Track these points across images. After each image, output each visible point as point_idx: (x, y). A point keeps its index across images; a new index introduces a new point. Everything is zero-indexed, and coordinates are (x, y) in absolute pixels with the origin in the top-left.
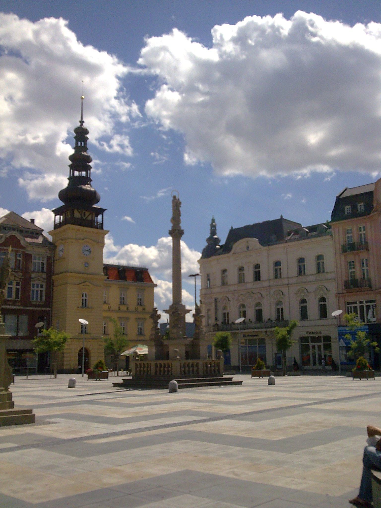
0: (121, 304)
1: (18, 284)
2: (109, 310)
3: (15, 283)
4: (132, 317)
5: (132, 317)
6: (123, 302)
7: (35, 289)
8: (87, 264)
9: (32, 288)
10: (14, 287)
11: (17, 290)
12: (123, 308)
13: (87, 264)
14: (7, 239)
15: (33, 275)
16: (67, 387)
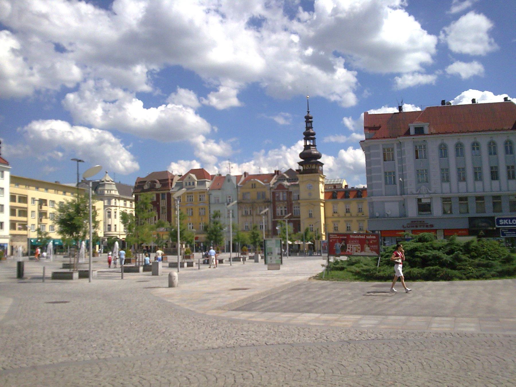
0: (347, 212)
1: (285, 208)
2: (339, 216)
3: (283, 207)
4: (355, 220)
5: (342, 220)
6: (348, 211)
7: (296, 209)
8: (310, 194)
9: (293, 209)
10: (283, 209)
11: (285, 211)
12: (348, 215)
13: (310, 194)
14: (278, 186)
15: (293, 202)
16: (61, 266)
